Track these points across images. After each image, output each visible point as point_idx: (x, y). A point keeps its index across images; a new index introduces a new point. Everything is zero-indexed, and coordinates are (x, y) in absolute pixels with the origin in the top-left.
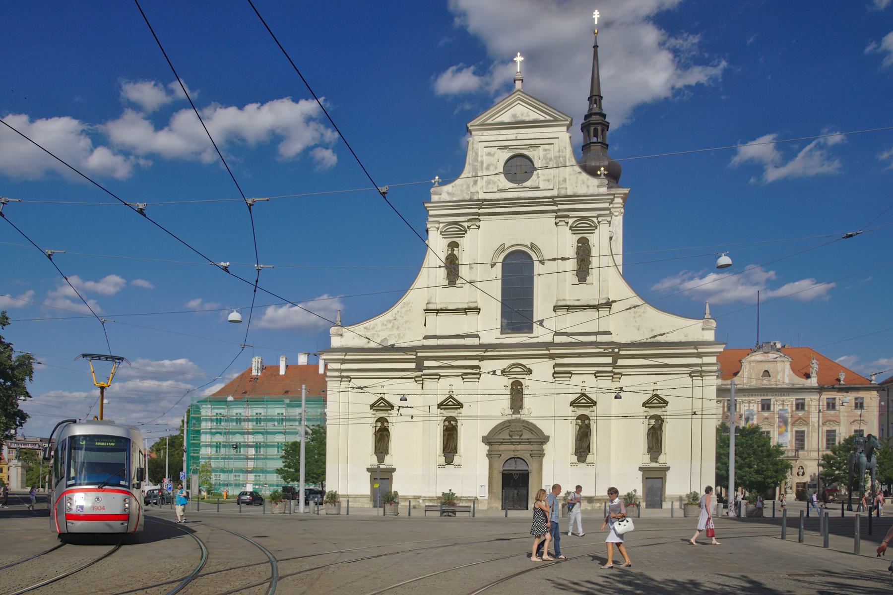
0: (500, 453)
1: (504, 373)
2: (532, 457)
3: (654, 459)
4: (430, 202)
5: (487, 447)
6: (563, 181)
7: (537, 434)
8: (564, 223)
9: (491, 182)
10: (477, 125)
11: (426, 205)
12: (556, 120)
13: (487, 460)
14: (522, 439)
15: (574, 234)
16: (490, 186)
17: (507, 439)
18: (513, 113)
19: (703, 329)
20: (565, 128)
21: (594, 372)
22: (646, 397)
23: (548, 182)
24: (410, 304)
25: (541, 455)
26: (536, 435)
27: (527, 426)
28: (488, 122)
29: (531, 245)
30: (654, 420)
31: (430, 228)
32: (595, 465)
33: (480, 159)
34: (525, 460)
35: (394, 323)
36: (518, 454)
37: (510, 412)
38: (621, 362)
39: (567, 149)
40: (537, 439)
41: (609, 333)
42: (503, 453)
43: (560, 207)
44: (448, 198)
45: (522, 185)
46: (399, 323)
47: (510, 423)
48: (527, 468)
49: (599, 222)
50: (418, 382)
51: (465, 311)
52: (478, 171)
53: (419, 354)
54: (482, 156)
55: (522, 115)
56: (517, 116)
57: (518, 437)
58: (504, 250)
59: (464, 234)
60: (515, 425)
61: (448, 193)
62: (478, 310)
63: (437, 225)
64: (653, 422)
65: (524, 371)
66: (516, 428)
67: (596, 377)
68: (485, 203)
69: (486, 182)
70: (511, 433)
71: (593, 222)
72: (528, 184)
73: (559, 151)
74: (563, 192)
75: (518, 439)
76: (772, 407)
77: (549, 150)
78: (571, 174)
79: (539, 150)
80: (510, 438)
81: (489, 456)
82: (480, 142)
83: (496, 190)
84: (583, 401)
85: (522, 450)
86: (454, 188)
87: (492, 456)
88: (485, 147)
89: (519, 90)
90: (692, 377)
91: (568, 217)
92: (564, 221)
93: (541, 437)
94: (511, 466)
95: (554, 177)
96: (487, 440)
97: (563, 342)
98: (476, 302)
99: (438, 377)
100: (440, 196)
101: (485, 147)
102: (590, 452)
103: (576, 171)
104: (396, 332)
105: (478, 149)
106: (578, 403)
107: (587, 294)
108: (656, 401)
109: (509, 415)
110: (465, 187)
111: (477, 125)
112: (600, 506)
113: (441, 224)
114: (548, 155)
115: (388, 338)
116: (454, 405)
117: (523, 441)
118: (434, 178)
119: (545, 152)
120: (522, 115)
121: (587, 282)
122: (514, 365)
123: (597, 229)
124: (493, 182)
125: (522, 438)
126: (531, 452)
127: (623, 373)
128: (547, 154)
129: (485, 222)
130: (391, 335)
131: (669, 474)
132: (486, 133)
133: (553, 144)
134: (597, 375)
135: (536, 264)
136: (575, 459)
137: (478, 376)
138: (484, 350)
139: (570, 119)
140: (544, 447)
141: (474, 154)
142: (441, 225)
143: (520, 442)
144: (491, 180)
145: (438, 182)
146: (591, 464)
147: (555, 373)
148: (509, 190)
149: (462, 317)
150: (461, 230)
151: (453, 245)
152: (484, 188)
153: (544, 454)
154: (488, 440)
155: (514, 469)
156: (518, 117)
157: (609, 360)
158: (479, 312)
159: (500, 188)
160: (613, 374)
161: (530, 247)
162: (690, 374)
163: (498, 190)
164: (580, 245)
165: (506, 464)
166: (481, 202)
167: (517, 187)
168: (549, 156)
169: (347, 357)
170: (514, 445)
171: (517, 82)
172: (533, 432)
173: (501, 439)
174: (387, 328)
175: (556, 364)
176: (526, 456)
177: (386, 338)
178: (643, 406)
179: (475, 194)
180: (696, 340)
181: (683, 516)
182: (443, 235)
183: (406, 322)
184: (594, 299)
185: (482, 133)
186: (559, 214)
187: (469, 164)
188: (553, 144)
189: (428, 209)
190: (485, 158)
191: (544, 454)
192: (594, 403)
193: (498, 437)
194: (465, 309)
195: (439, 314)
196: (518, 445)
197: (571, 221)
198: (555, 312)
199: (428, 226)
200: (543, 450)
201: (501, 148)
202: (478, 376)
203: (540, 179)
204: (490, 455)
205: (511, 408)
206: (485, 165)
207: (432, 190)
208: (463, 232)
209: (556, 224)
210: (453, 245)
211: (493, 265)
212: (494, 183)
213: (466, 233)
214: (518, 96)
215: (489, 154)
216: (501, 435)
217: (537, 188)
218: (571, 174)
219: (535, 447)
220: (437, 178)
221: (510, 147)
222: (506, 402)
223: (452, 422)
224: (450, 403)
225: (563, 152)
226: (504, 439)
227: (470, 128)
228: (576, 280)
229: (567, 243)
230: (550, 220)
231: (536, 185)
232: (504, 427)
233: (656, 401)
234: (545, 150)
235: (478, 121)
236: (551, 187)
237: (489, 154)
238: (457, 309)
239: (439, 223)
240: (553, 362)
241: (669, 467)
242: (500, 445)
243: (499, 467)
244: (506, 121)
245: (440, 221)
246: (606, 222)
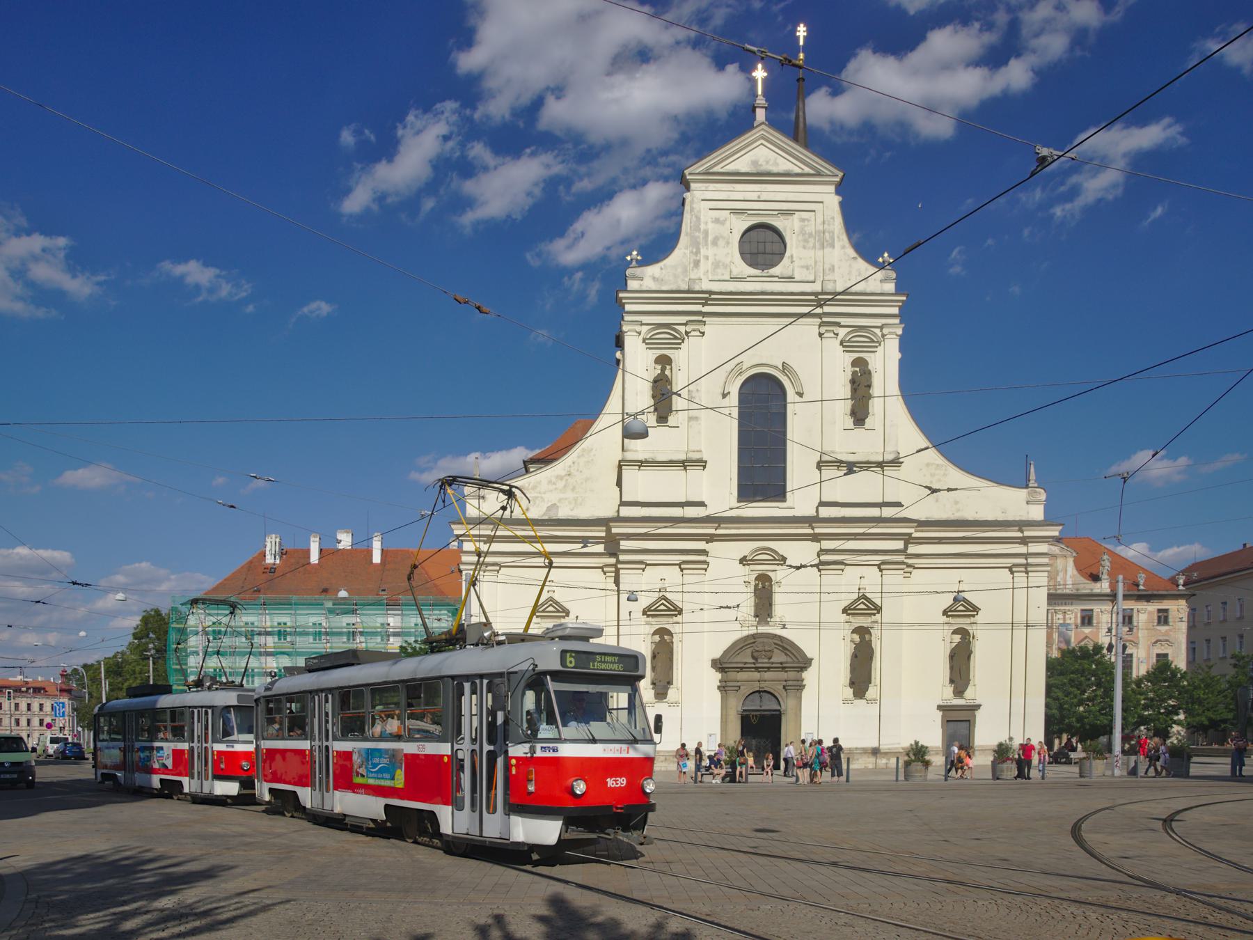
0: (739, 684)
1: (743, 561)
2: (786, 690)
3: (959, 692)
4: (625, 290)
5: (719, 676)
6: (830, 269)
7: (795, 656)
8: (832, 335)
9: (721, 264)
10: (699, 174)
11: (621, 295)
12: (819, 174)
13: (717, 695)
15: (847, 351)
16: (719, 271)
17: (751, 663)
18: (753, 158)
19: (1028, 503)
20: (832, 188)
21: (878, 563)
22: (948, 601)
23: (808, 269)
24: (594, 450)
25: (801, 687)
26: (792, 657)
27: (781, 644)
28: (715, 169)
29: (783, 366)
30: (960, 636)
31: (627, 332)
32: (878, 702)
33: (702, 227)
34: (776, 694)
35: (567, 480)
36: (766, 686)
37: (754, 621)
38: (913, 549)
39: (835, 219)
40: (793, 663)
41: (899, 504)
42: (743, 685)
43: (827, 309)
44: (654, 287)
45: (768, 272)
46: (576, 481)
47: (755, 639)
48: (778, 708)
49: (883, 336)
50: (607, 574)
51: (684, 464)
52: (701, 247)
53: (614, 530)
54: (706, 223)
55: (767, 162)
56: (760, 163)
57: (767, 661)
58: (741, 372)
59: (680, 344)
60: (763, 642)
61: (654, 278)
62: (702, 463)
63: (638, 328)
64: (957, 638)
65: (775, 560)
67: (881, 570)
68: (713, 297)
69: (713, 263)
70: (755, 654)
71: (875, 335)
72: (776, 271)
73: (824, 223)
74: (829, 287)
75: (766, 663)
76: (1135, 619)
77: (808, 220)
78: (841, 260)
79: (793, 220)
80: (754, 661)
81: (722, 689)
82: (703, 200)
83: (728, 278)
84: (862, 606)
85: (772, 680)
86: (663, 271)
88: (710, 209)
89: (763, 123)
90: (1012, 573)
91: (838, 325)
92: (833, 331)
93: (801, 660)
94: (754, 705)
95: (816, 262)
96: (718, 665)
97: (833, 516)
98: (700, 451)
99: (643, 566)
100: (642, 282)
101: (710, 209)
102: (870, 683)
103: (848, 256)
104: (570, 495)
105: (700, 211)
106: (855, 609)
107: (863, 445)
108: (962, 607)
109: (752, 626)
110: (680, 270)
111: (699, 174)
112: (887, 763)
113: (643, 326)
114: (806, 229)
115: (558, 504)
116: (669, 610)
117: (774, 665)
118: (631, 254)
119: (802, 223)
120: (767, 162)
121: (866, 426)
122: (759, 550)
123: (880, 345)
124: (723, 265)
125: (772, 660)
126: (784, 683)
127: (916, 566)
128: (805, 226)
129: (713, 327)
130: (563, 499)
131: (979, 715)
132: (712, 186)
133: (814, 211)
134: (882, 567)
135: (791, 395)
136: (849, 692)
137: (705, 566)
138: (717, 525)
139: (841, 174)
140: (804, 675)
141: (694, 219)
142: (644, 329)
143: (769, 668)
144: (720, 261)
145: (637, 260)
147: (821, 563)
148: (748, 279)
149: (677, 474)
150: (676, 338)
151: (664, 361)
152: (710, 271)
153: (805, 685)
154: (721, 665)
155: (759, 708)
156: (761, 165)
157: (899, 545)
158: (704, 467)
159: (734, 275)
160: (905, 566)
161: (781, 368)
162: (1010, 569)
163: (731, 278)
164: (858, 369)
165: (747, 702)
166: (707, 295)
167: (760, 275)
168: (808, 230)
169: (498, 533)
170: (759, 672)
171: (757, 110)
172: (788, 653)
173: (742, 663)
174: (556, 489)
175: (822, 552)
176: (777, 689)
177: (555, 504)
178: (943, 615)
179: (697, 281)
180: (1017, 519)
181: (990, 776)
182: (647, 344)
183: (587, 480)
184: (877, 453)
185: (706, 187)
186: (824, 319)
187: (687, 234)
188: (814, 211)
189: (624, 301)
190: (711, 226)
192: (878, 609)
193: (735, 660)
194: (683, 462)
195: (641, 468)
196: (766, 672)
197: (842, 332)
198: (820, 470)
199: (625, 328)
200: (802, 680)
201: (735, 211)
202: (705, 566)
203: (796, 264)
204: (724, 687)
205: (756, 616)
206: (710, 238)
207: (629, 272)
208: (677, 341)
209: (821, 335)
210: (664, 361)
211: (724, 396)
212: (725, 266)
213: (683, 342)
214: (762, 132)
215: (717, 221)
216: (739, 656)
217: (790, 278)
218: (841, 260)
219: (792, 675)
220: (635, 253)
221: (749, 212)
222: (747, 603)
223: (666, 637)
224: (662, 607)
225: (829, 225)
226: (746, 663)
227: (688, 177)
228: (849, 422)
229: (839, 366)
230: (809, 328)
231: (788, 273)
232: (746, 643)
233: (962, 607)
234: (803, 220)
235: (701, 167)
236: (812, 278)
237: (717, 221)
238: (671, 462)
239: (642, 324)
240: (815, 547)
241: (980, 706)
242: (738, 672)
243: (736, 706)
244: (743, 170)
245: (644, 322)
246: (895, 336)
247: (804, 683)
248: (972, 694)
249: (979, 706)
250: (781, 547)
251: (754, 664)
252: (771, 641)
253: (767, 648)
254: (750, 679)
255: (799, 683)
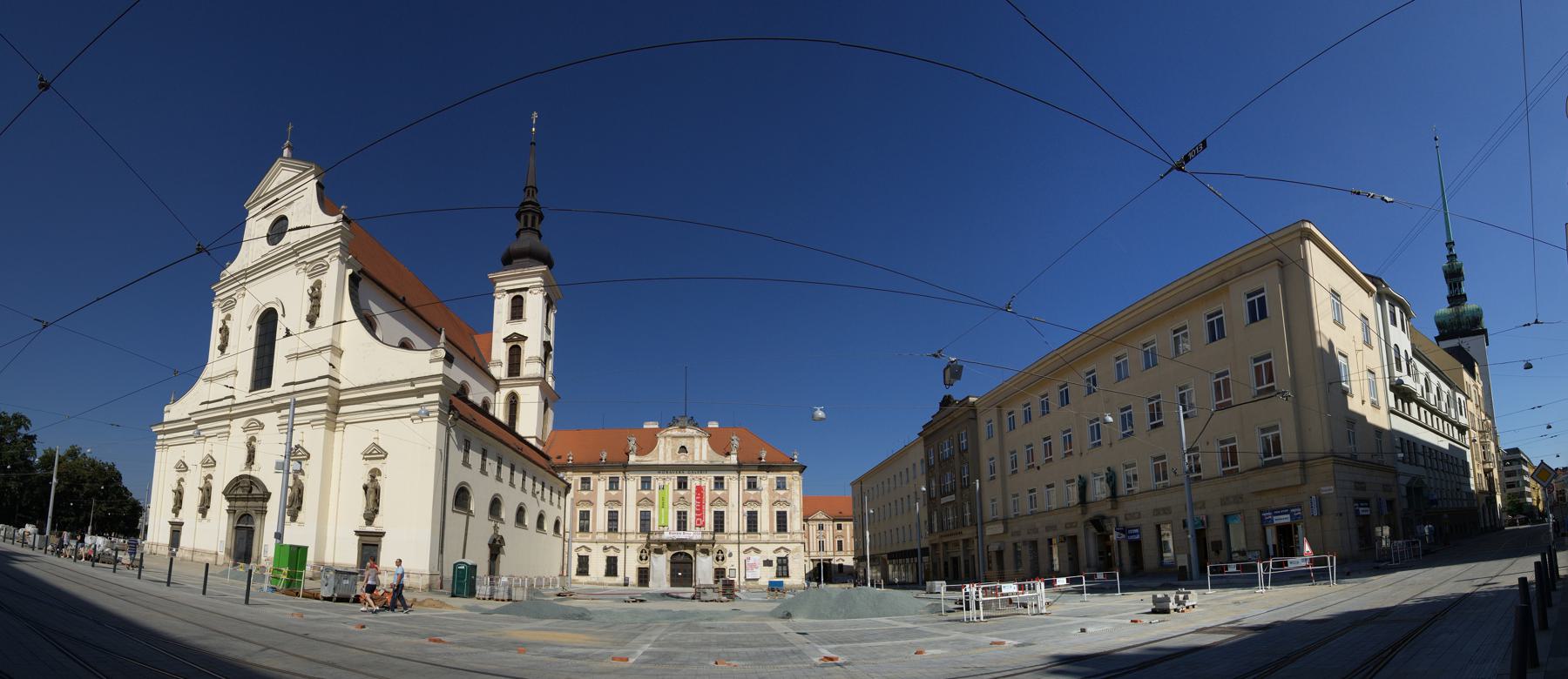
5: (228, 504)
25: (263, 512)
96: (223, 493)
146: (301, 524)
191: (266, 512)
219: (260, 503)
248: (379, 523)
249: (382, 534)
250: (260, 417)
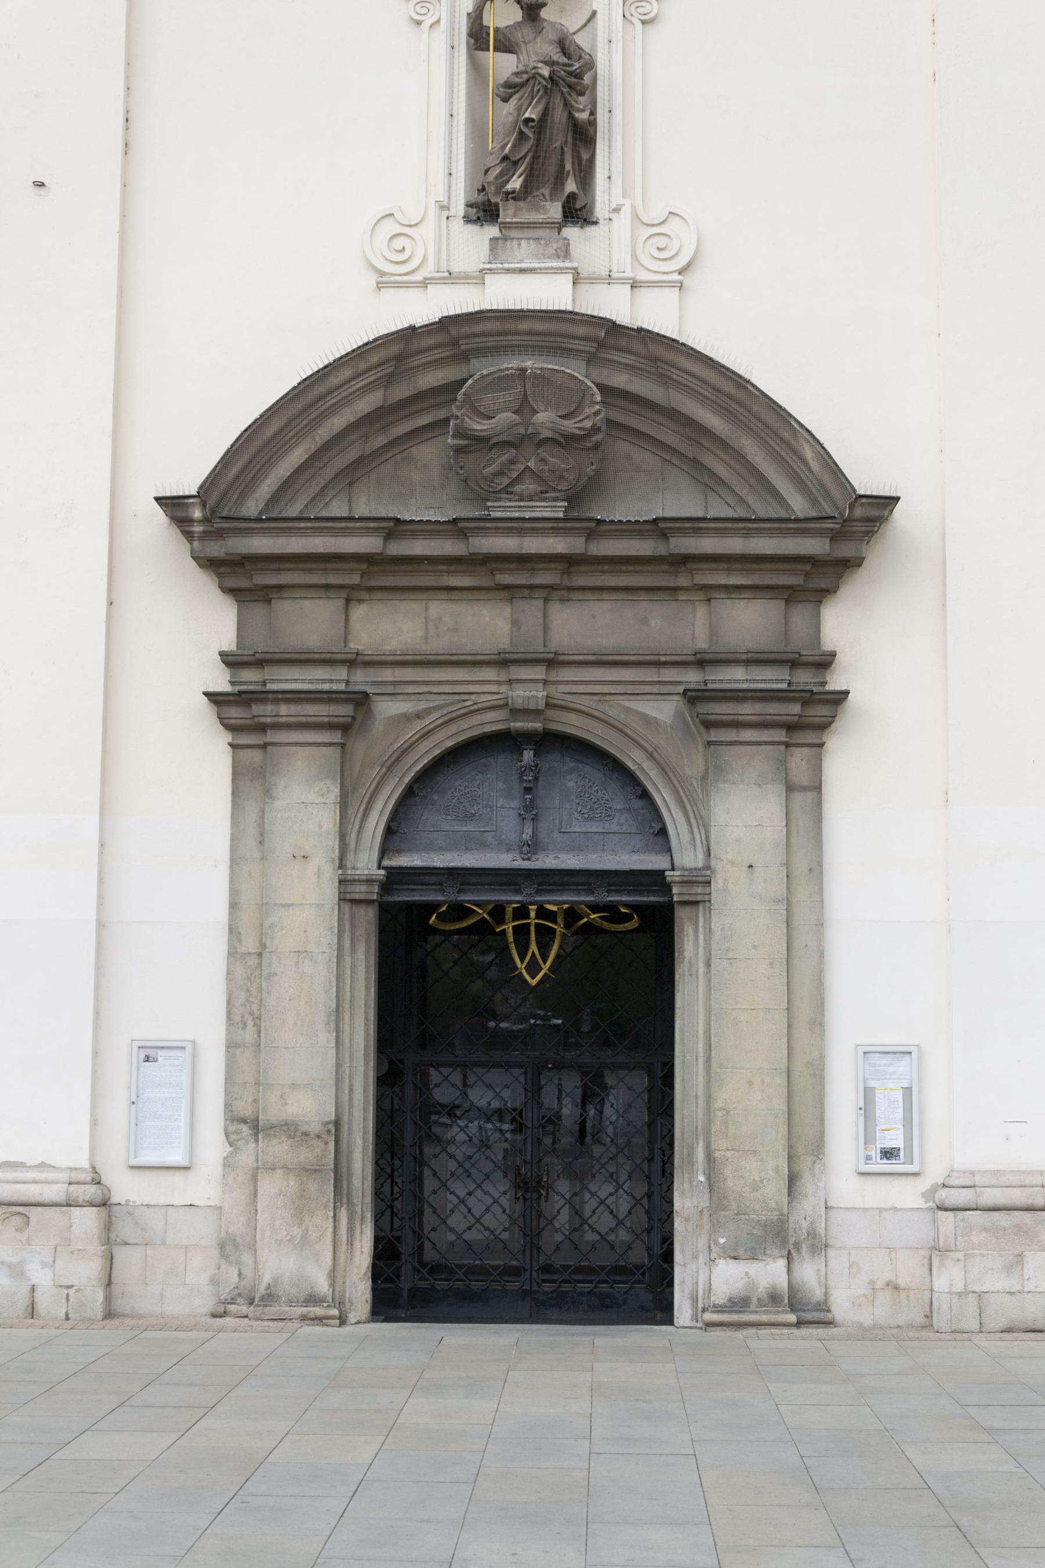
0: (361, 679)
14: (597, 529)
34: (634, 759)
57: (553, 509)
66: (524, 407)
87: (265, 711)
126: (692, 677)
143: (569, 562)
200: (825, 662)
232: (402, 391)
242: (351, 596)
247: (835, 683)
251: (456, 528)
252: (575, 369)
253: (544, 418)
254: (438, 645)
255: (804, 678)
